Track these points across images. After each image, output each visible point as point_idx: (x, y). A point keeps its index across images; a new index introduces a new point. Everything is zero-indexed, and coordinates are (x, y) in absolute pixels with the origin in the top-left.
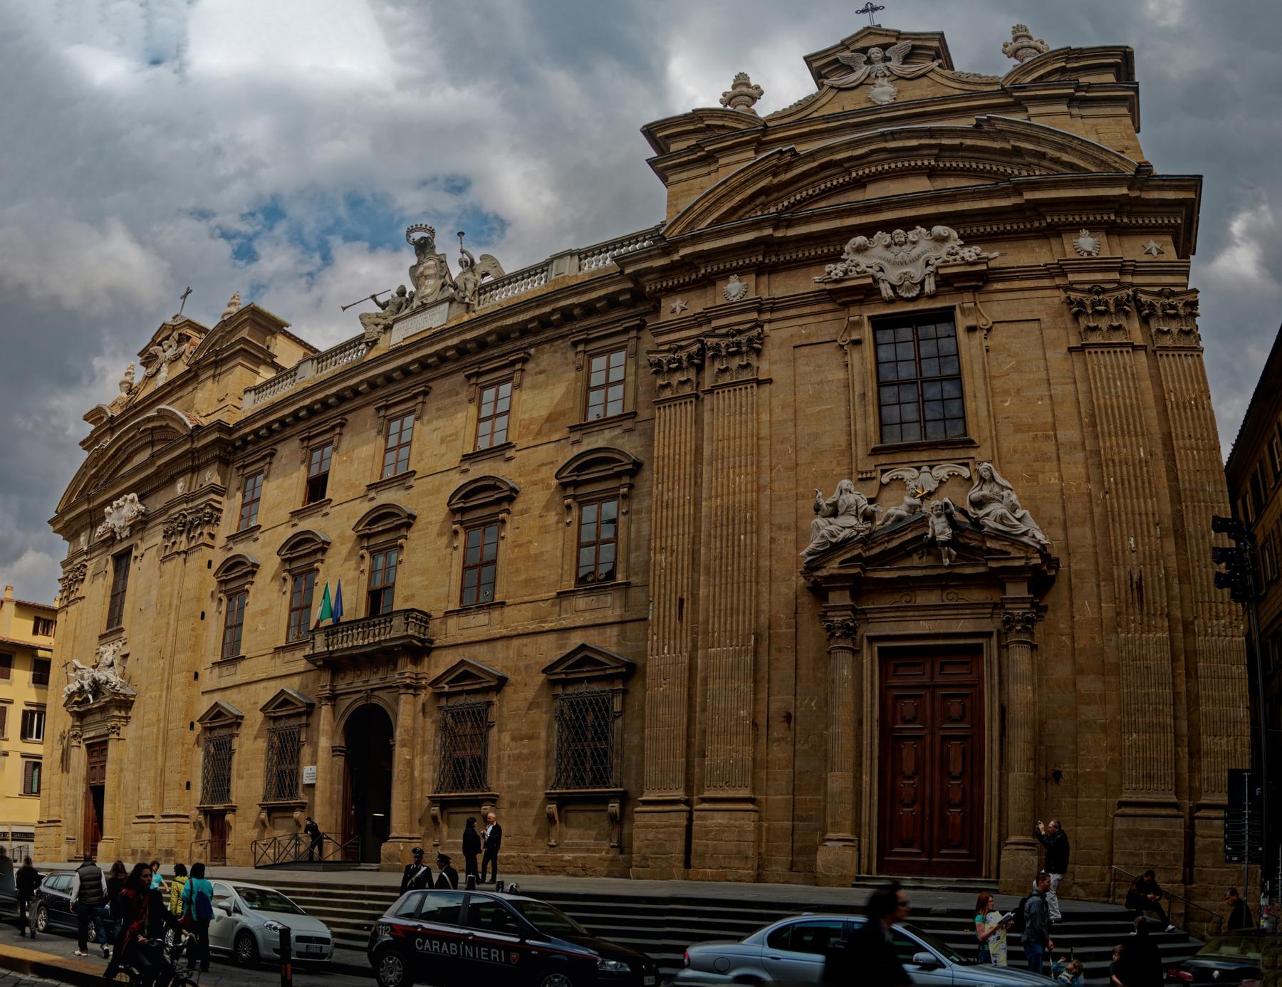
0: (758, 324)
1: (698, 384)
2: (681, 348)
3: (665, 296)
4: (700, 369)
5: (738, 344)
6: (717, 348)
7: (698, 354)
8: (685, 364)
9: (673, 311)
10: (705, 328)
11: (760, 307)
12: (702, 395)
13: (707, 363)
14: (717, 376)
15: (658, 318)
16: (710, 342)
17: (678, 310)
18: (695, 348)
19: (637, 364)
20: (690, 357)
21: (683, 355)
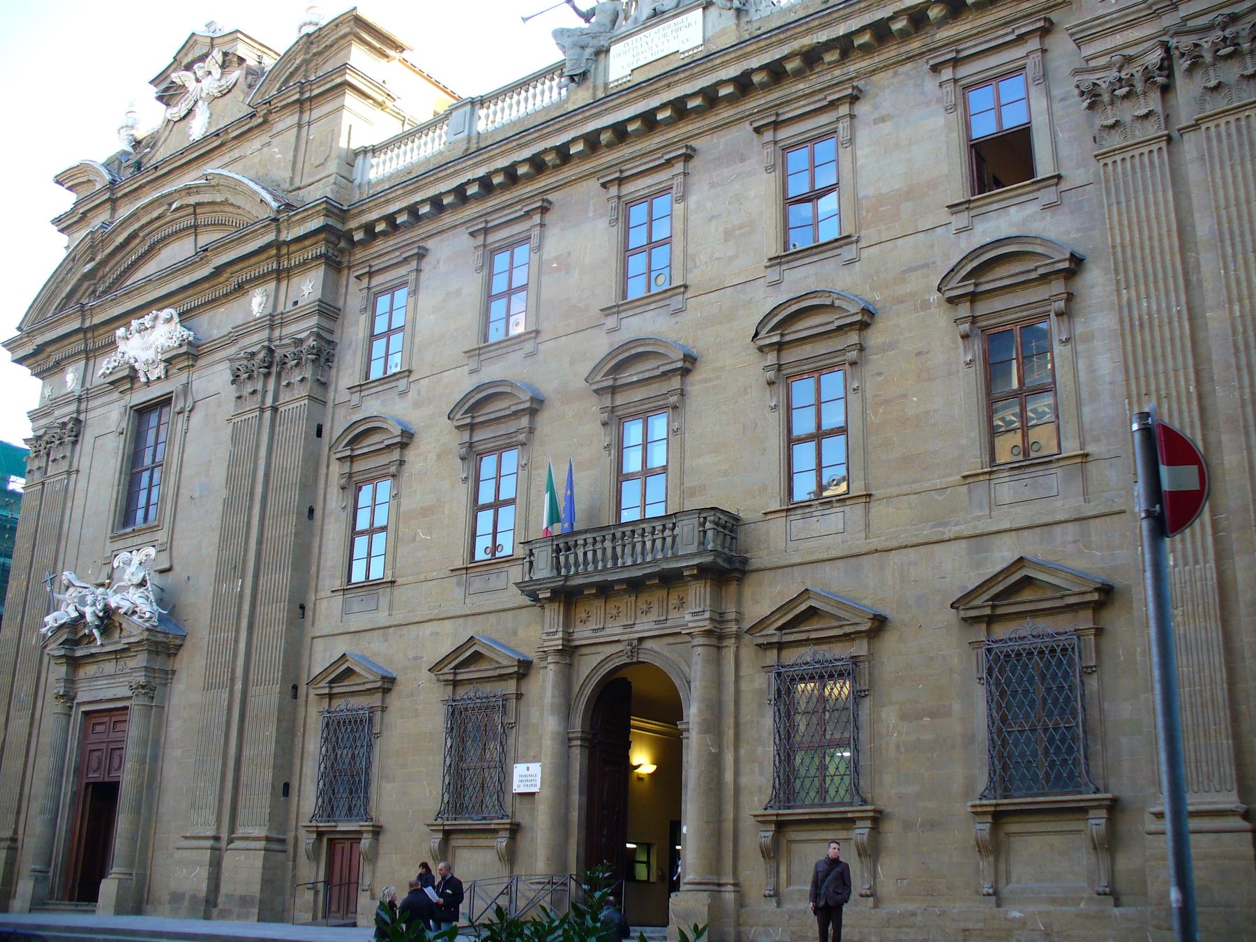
1: (1167, 117)
2: (1129, 60)
4: (1166, 89)
7: (1160, 68)
8: (1139, 87)
12: (1175, 135)
14: (1202, 101)
18: (1155, 57)
19: (1048, 95)
21: (1136, 69)
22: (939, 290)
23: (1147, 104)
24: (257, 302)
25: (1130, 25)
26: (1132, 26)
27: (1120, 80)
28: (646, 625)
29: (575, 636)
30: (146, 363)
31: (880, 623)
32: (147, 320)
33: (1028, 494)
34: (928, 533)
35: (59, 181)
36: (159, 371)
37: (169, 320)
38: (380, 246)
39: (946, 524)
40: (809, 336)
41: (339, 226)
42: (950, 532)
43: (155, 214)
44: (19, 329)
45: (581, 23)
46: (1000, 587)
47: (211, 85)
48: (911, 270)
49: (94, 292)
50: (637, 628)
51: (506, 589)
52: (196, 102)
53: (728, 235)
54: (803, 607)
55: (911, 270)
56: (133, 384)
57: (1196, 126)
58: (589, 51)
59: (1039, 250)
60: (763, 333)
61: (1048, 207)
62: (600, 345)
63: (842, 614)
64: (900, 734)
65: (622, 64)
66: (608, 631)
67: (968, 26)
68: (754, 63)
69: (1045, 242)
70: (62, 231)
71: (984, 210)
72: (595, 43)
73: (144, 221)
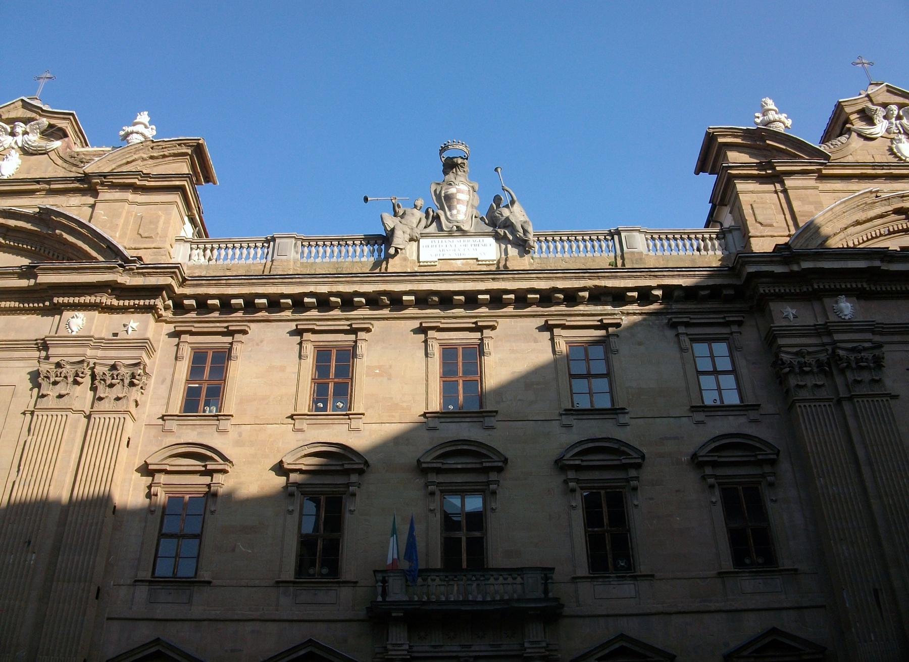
0: (879, 346)
9: (786, 318)
11: (873, 328)
25: (804, 335)
27: (805, 363)
29: (415, 649)
50: (473, 649)
54: (617, 646)
61: (751, 421)
66: (448, 649)
71: (713, 414)
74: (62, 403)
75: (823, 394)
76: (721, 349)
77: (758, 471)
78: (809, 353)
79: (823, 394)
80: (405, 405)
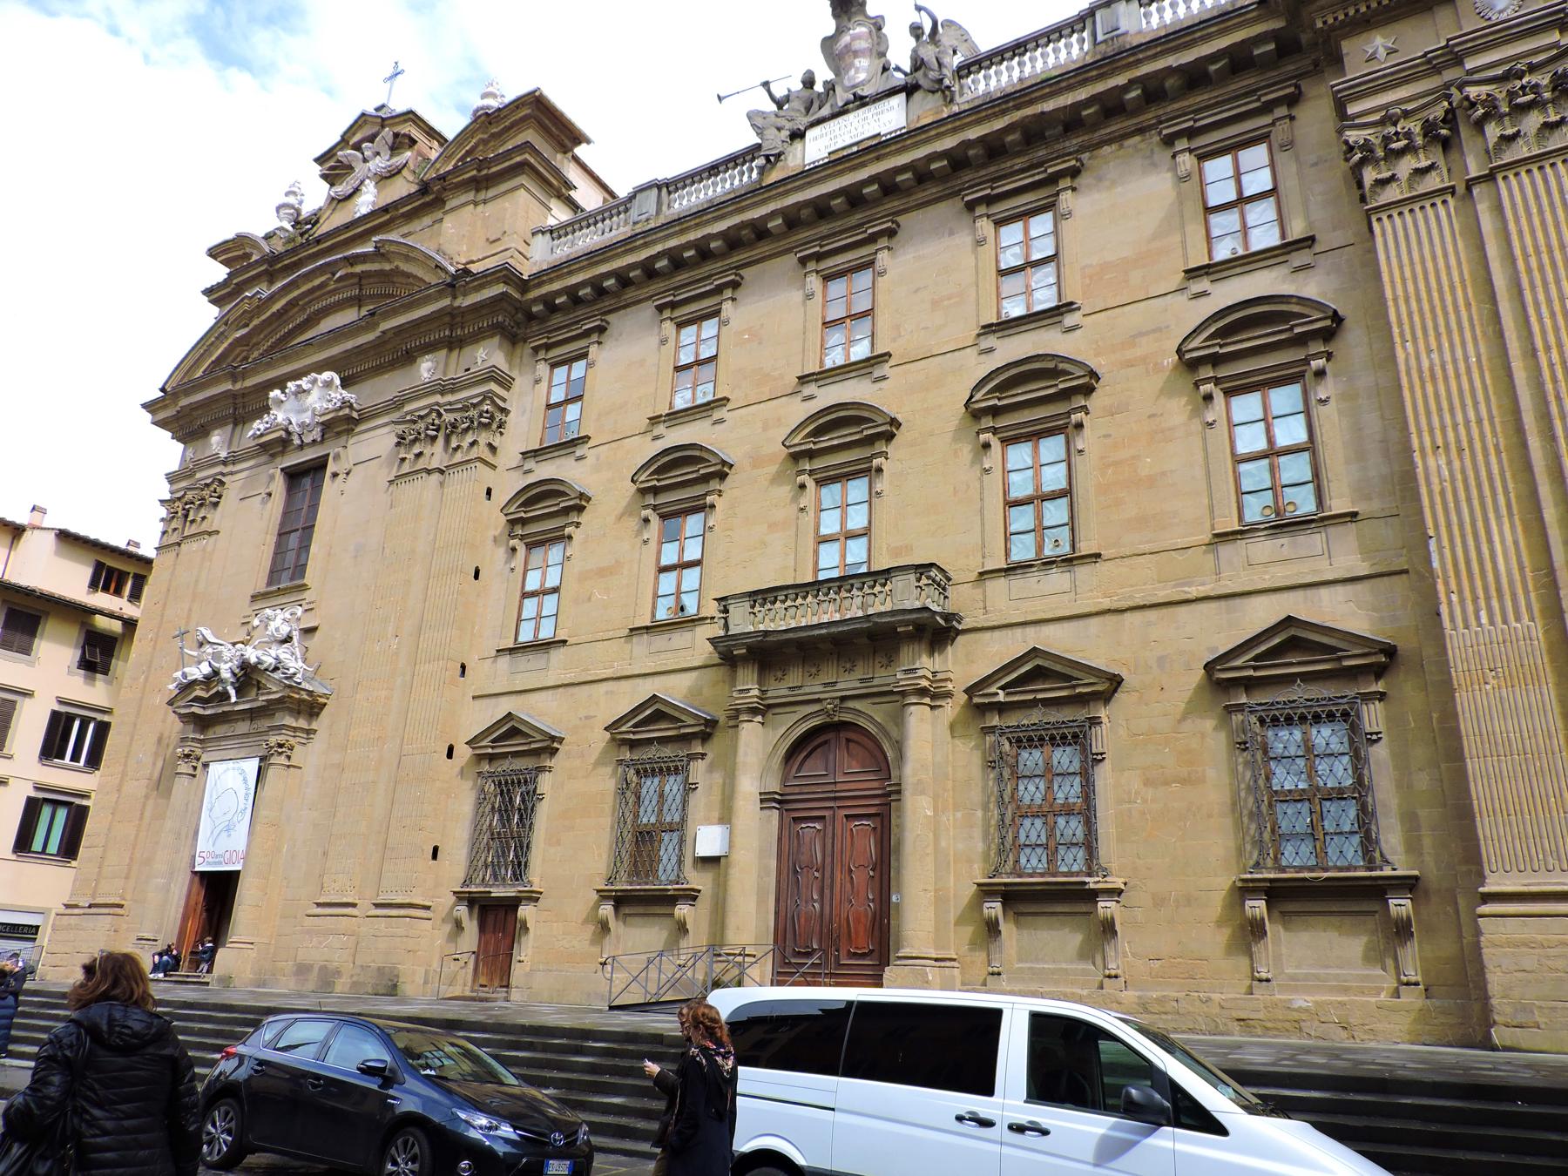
3: (1346, 36)
5: (1535, 88)
6: (1491, 102)
7: (1444, 121)
10: (1450, 75)
13: (1465, 132)
15: (1342, 72)
16: (1473, 91)
17: (1382, 53)
18: (1438, 112)
19: (1297, 159)
20: (1429, 128)
22: (1179, 351)
23: (1427, 158)
24: (426, 368)
25: (1406, 81)
26: (1407, 82)
27: (1397, 133)
28: (848, 682)
29: (769, 694)
30: (302, 425)
31: (1116, 682)
32: (304, 383)
33: (1287, 552)
34: (1162, 595)
35: (214, 253)
36: (316, 434)
37: (328, 384)
38: (557, 319)
39: (1189, 584)
40: (1033, 397)
41: (516, 295)
42: (1194, 591)
43: (317, 282)
44: (163, 390)
45: (774, 107)
46: (1263, 648)
47: (379, 164)
48: (1141, 334)
49: (246, 358)
50: (839, 686)
51: (697, 646)
52: (362, 182)
53: (935, 304)
55: (1141, 334)
56: (285, 447)
57: (1490, 177)
58: (785, 134)
59: (1296, 309)
60: (978, 396)
62: (798, 411)
63: (1075, 673)
64: (1145, 801)
65: (819, 145)
66: (807, 690)
67: (1206, 97)
68: (973, 134)
69: (1302, 301)
70: (213, 302)
72: (788, 125)
73: (304, 288)
74: (421, 464)
75: (1433, 182)
76: (1257, 155)
77: (1299, 354)
78: (1406, 114)
79: (1433, 182)
80: (776, 374)
